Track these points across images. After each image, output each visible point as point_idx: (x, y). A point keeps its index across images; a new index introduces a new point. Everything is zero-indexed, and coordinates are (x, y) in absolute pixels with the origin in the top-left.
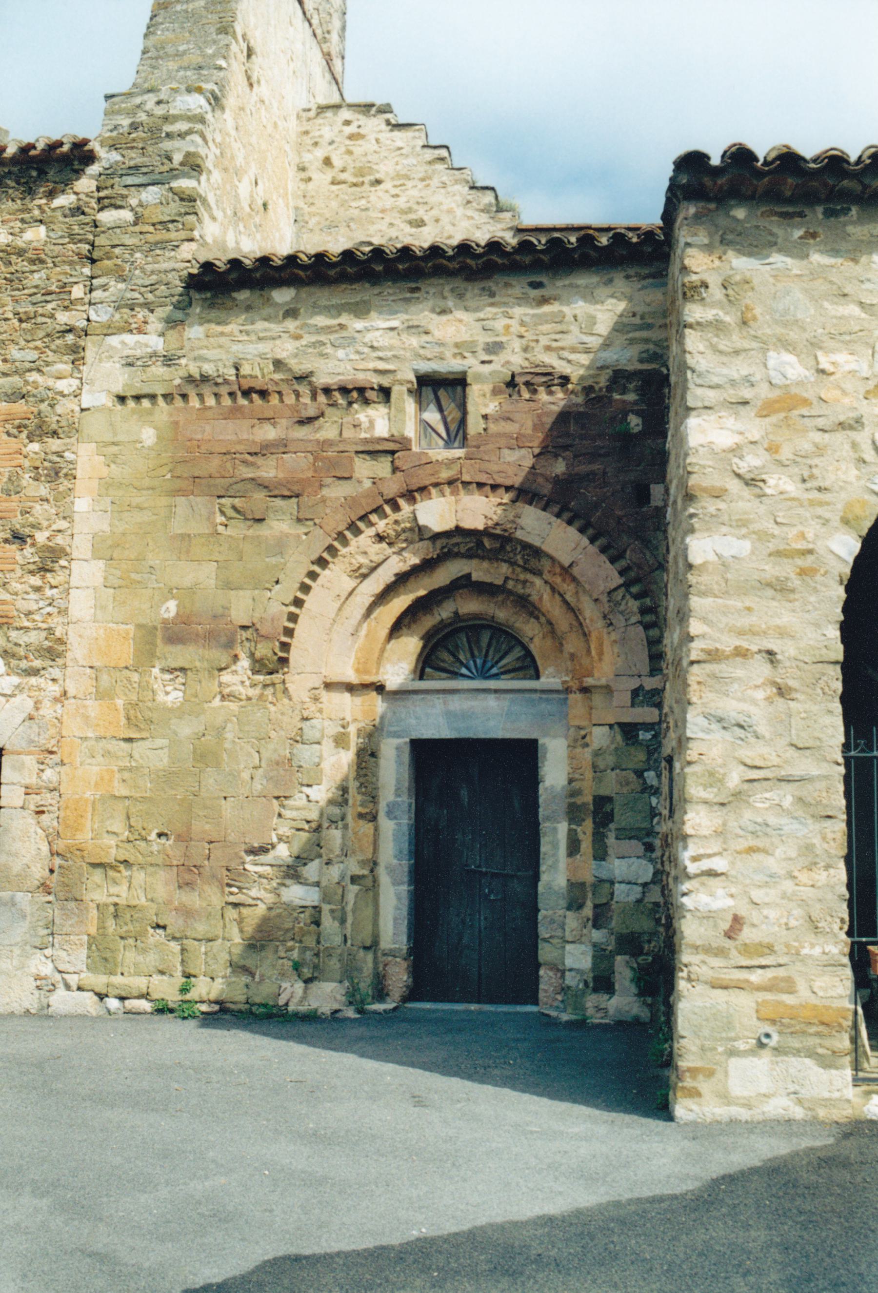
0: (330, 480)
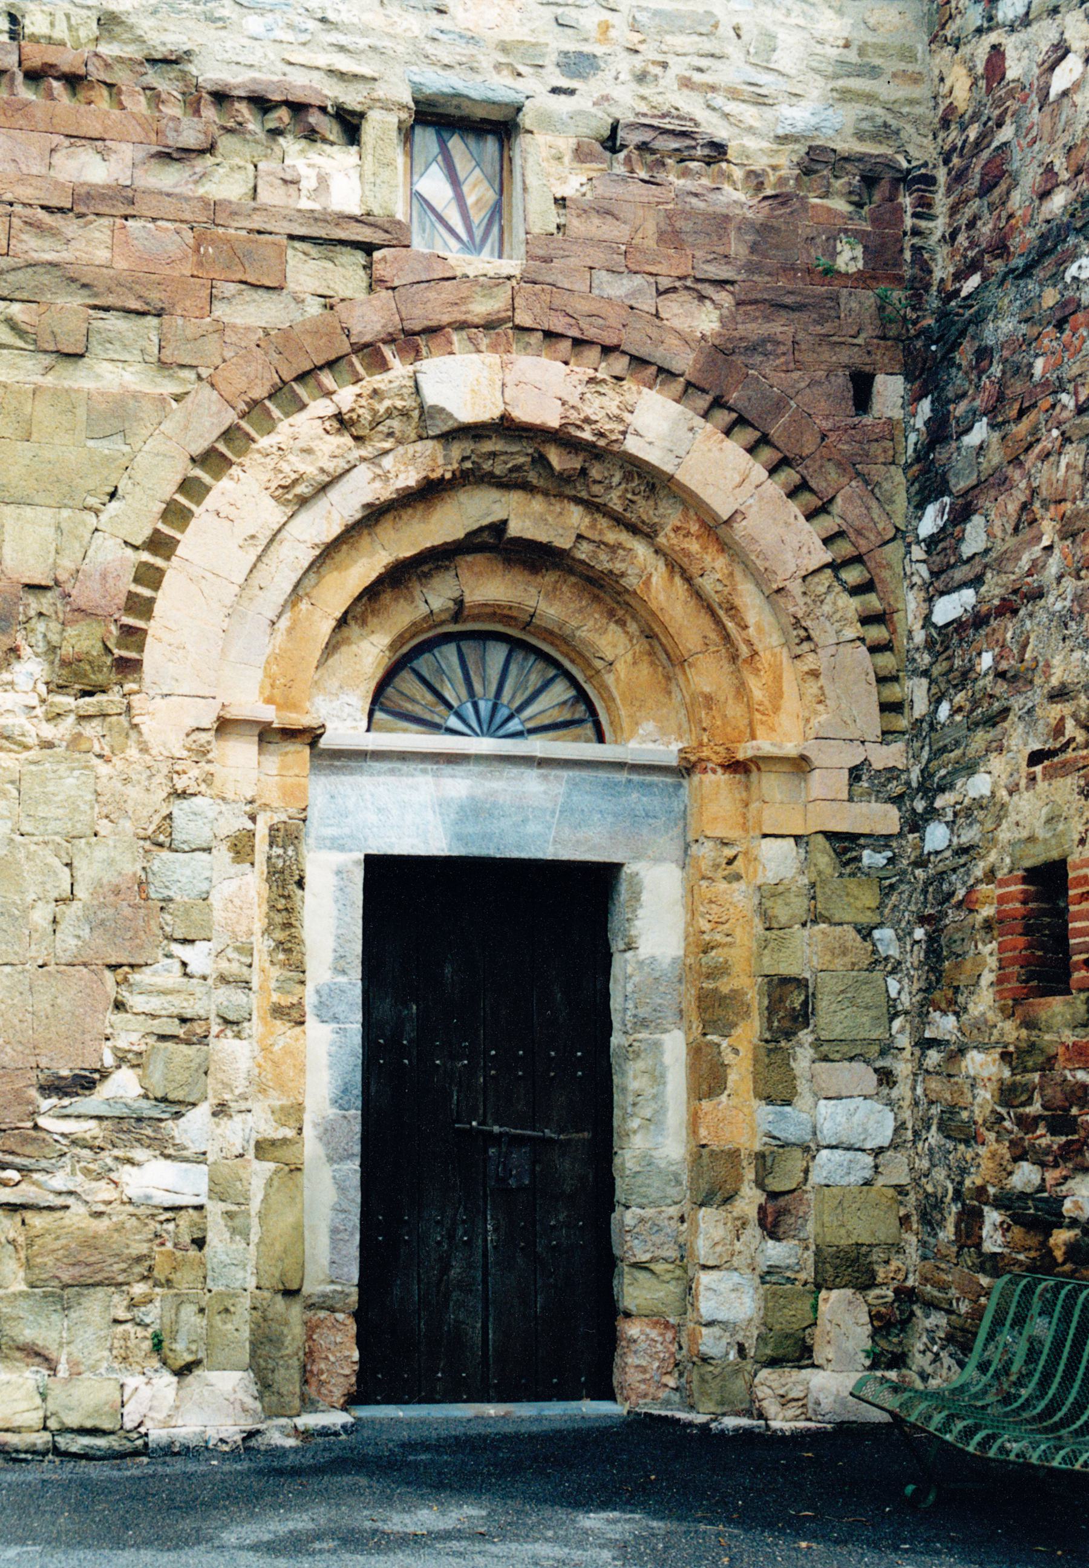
0: (233, 288)
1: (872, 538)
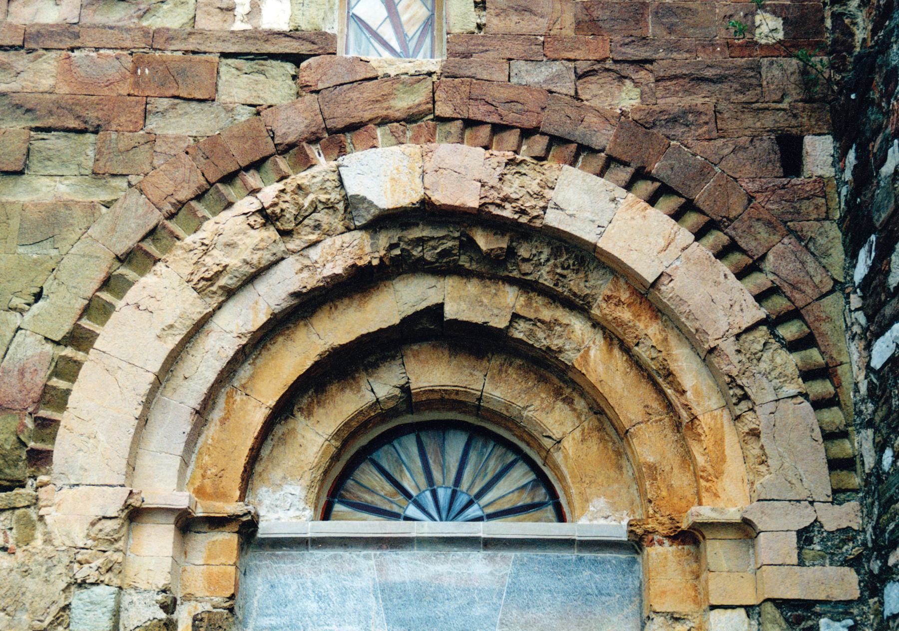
0: (165, 103)
1: (809, 291)
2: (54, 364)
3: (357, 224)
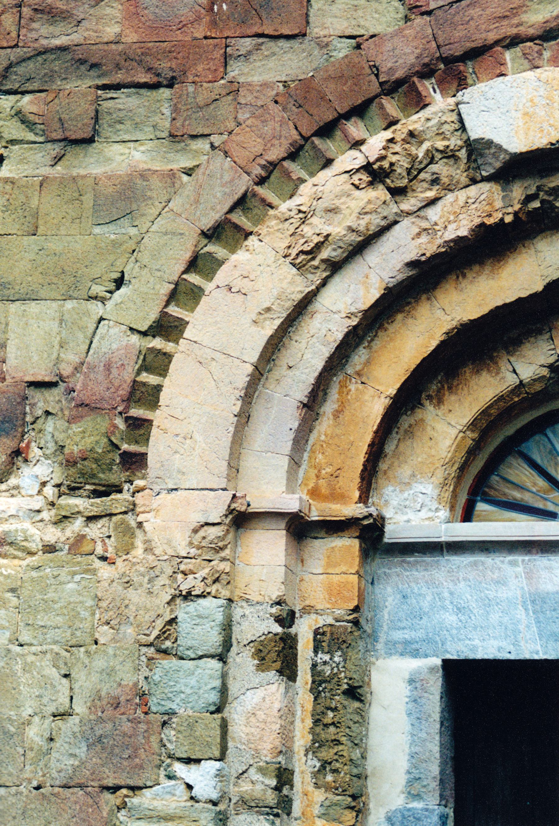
0: (247, 43)
2: (142, 357)
3: (484, 174)
